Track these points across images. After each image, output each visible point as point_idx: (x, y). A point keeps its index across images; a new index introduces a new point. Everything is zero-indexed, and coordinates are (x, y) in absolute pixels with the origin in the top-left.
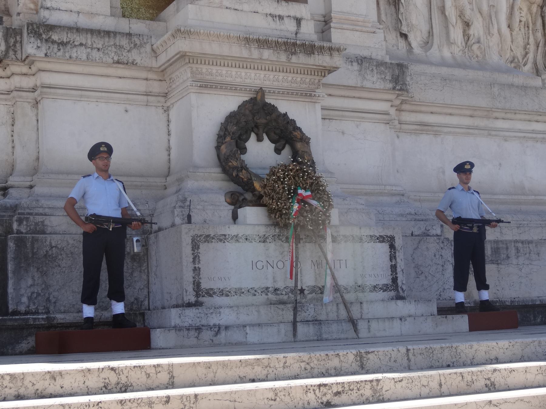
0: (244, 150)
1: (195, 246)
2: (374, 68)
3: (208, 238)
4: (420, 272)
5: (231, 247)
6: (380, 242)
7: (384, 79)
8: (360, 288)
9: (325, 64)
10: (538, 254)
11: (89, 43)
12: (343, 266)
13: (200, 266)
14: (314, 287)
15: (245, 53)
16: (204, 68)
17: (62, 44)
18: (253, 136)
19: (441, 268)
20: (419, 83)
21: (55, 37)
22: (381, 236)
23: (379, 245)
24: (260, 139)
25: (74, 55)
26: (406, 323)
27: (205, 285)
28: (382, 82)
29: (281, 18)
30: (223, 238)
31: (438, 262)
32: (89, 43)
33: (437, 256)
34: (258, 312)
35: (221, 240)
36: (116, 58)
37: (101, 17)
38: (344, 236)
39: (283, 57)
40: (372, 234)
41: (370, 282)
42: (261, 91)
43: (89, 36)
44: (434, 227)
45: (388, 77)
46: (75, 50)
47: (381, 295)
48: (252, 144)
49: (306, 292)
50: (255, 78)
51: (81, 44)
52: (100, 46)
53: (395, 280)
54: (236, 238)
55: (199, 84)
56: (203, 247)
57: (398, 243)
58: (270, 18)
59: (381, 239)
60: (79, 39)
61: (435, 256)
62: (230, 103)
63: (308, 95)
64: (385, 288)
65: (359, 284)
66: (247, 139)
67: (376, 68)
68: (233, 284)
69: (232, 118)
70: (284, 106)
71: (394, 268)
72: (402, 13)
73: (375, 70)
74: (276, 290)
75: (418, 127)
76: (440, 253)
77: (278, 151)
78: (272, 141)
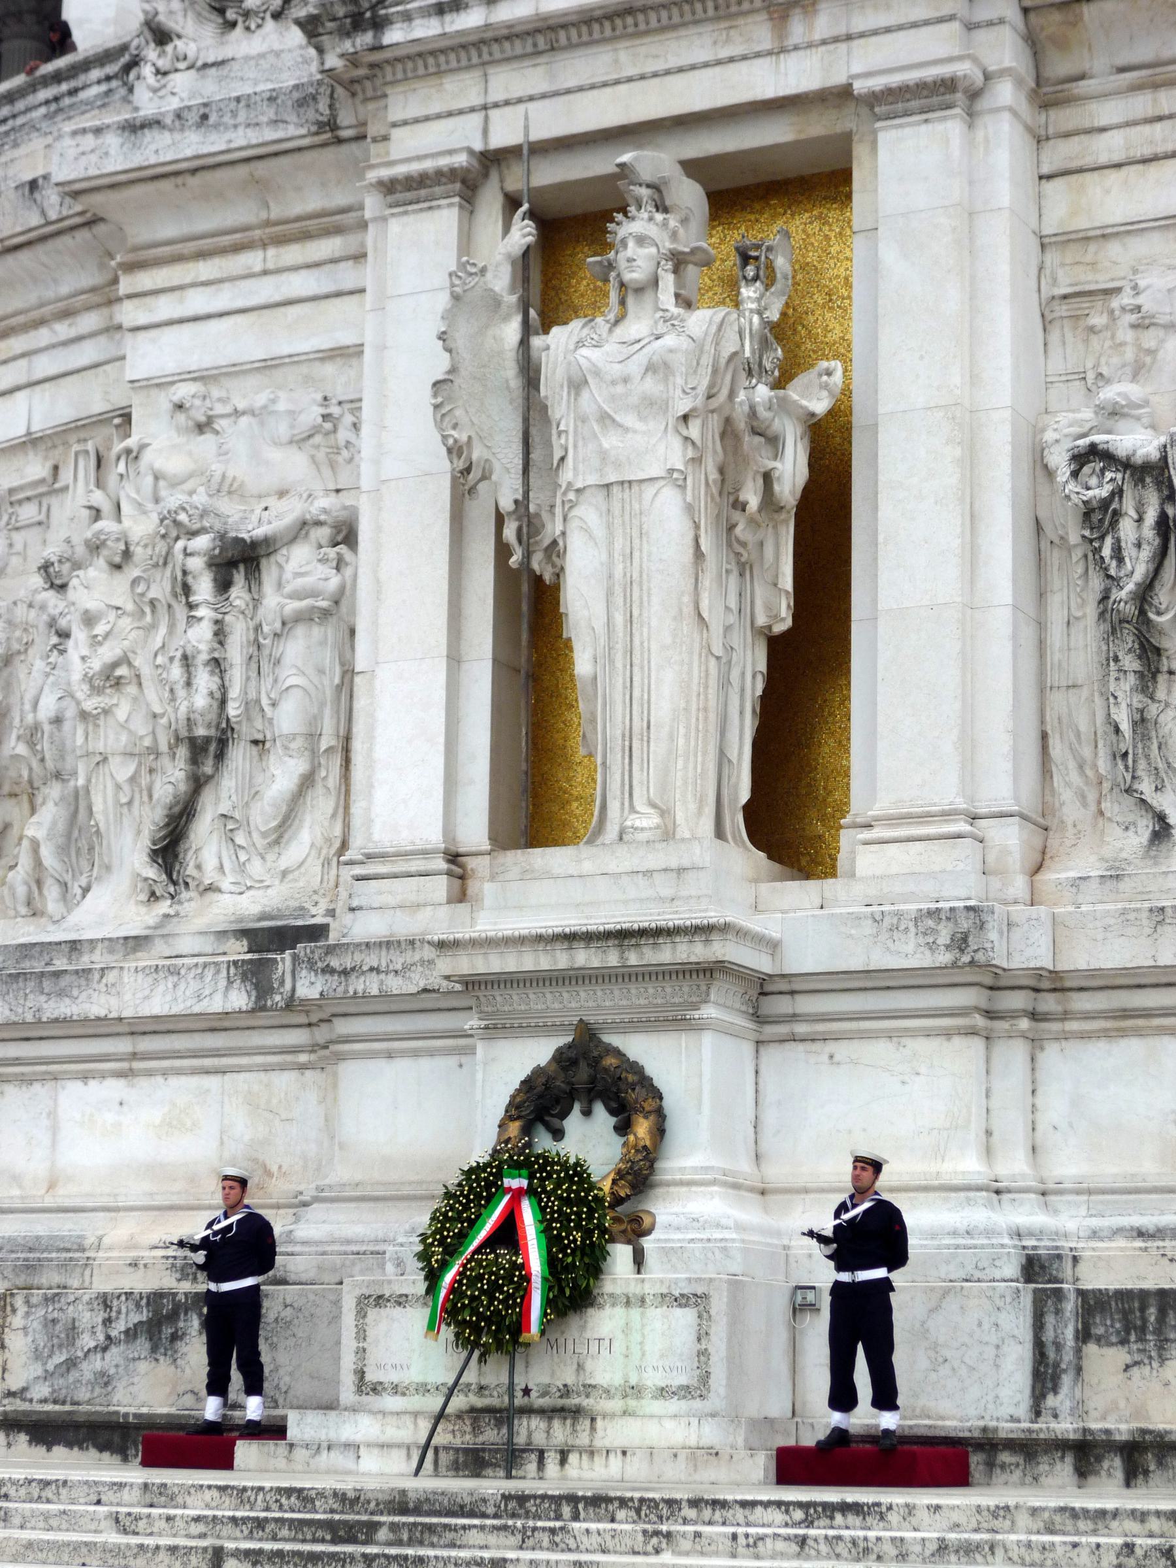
0: (558, 1134)
1: (361, 1314)
2: (911, 925)
4: (941, 1360)
6: (680, 1306)
7: (932, 947)
8: (634, 1391)
9: (693, 959)
11: (384, 964)
12: (605, 1352)
13: (365, 1345)
14: (549, 1385)
17: (345, 973)
18: (577, 1107)
19: (993, 1351)
20: (1091, 926)
21: (335, 963)
22: (682, 1295)
23: (678, 1312)
24: (587, 1113)
25: (360, 988)
26: (635, 1459)
27: (371, 1376)
28: (928, 953)
29: (648, 873)
31: (986, 1339)
32: (384, 964)
33: (986, 1326)
34: (416, 1424)
35: (400, 1304)
36: (422, 985)
37: (429, 908)
38: (611, 1295)
40: (665, 1291)
41: (653, 1379)
43: (384, 953)
44: (997, 1263)
45: (944, 938)
46: (362, 979)
47: (674, 1405)
48: (574, 1123)
49: (533, 1394)
51: (372, 969)
52: (399, 967)
53: (705, 1378)
55: (483, 1023)
56: (372, 1313)
58: (625, 880)
59: (682, 1301)
60: (371, 960)
61: (980, 1324)
64: (685, 1392)
65: (633, 1382)
66: (564, 1114)
67: (916, 926)
71: (703, 1354)
72: (1126, 754)
73: (913, 930)
74: (481, 1388)
75: (1109, 1024)
76: (993, 1319)
78: (612, 1112)
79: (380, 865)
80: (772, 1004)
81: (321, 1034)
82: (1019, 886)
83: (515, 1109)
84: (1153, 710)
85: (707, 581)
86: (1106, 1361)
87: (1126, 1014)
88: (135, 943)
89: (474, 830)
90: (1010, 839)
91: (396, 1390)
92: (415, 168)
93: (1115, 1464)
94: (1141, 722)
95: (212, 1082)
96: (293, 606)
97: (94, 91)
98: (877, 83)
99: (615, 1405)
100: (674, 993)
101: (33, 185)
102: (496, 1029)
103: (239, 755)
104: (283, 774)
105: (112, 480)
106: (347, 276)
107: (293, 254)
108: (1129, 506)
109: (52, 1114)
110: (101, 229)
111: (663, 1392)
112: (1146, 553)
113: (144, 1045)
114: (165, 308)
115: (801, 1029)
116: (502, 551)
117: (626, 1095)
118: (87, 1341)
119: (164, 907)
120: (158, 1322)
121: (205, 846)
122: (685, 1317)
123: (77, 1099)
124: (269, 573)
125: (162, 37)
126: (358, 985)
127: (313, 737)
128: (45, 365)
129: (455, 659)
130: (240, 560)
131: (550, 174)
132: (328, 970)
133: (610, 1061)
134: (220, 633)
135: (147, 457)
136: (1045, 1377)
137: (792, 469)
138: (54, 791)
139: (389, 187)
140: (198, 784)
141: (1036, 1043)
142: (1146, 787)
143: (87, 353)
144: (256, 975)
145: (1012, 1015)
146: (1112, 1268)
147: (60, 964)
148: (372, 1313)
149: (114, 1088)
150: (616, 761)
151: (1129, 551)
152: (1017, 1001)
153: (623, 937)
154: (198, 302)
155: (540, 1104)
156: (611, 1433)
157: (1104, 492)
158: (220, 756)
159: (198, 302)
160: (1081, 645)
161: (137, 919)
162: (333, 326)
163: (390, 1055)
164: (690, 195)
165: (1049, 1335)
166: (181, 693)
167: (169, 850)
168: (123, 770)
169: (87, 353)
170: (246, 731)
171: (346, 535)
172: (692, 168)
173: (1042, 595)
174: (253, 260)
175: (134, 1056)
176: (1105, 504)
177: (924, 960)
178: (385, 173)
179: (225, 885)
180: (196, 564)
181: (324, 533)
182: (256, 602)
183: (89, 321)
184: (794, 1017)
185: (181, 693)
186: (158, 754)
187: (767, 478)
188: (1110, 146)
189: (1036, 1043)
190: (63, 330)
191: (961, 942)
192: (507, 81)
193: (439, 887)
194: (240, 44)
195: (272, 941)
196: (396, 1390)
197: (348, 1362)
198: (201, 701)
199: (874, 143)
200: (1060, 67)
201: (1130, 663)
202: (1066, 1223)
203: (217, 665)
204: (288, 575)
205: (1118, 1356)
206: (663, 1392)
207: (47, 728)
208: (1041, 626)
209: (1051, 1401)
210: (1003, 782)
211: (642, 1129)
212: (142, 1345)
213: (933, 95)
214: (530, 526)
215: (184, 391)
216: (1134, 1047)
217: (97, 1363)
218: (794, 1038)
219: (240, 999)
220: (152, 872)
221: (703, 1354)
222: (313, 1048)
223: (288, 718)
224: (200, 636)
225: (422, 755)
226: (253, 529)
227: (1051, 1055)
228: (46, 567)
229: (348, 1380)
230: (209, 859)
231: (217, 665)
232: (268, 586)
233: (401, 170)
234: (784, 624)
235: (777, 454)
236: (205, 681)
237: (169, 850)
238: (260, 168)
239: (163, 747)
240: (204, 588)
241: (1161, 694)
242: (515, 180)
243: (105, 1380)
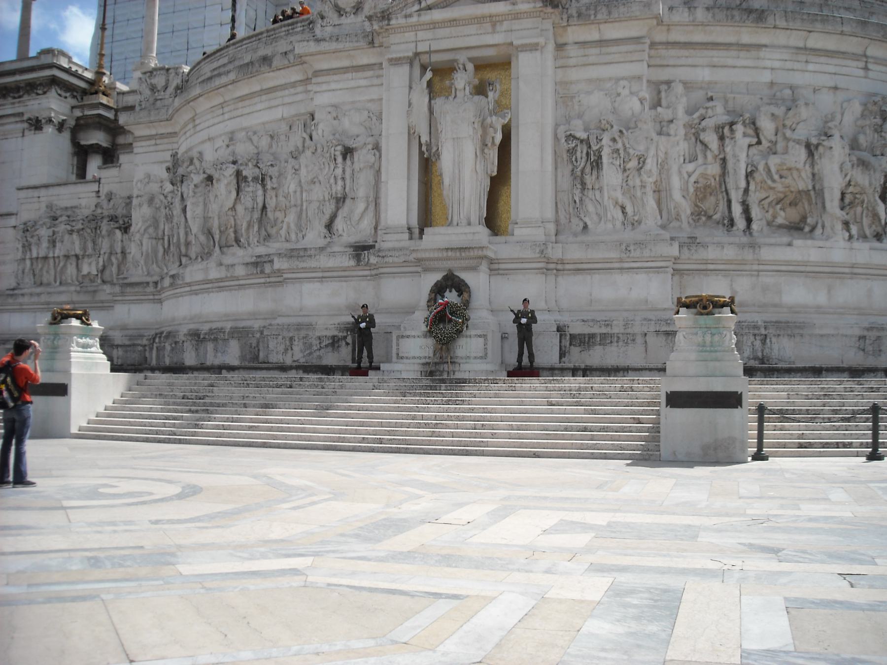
0: (443, 297)
1: (398, 340)
3: (403, 337)
5: (411, 340)
10: (634, 340)
15: (440, 255)
16: (427, 263)
24: (450, 291)
30: (408, 337)
39: (458, 254)
41: (473, 355)
42: (450, 270)
45: (538, 251)
47: (479, 361)
48: (447, 294)
50: (449, 264)
53: (486, 354)
54: (414, 337)
56: (400, 340)
57: (489, 337)
59: (480, 336)
62: (438, 277)
63: (474, 269)
64: (481, 358)
68: (411, 354)
69: (436, 284)
70: (463, 275)
71: (486, 348)
77: (459, 296)
79: (388, 230)
80: (495, 267)
81: (373, 272)
82: (553, 238)
83: (432, 291)
84: (584, 198)
85: (478, 162)
86: (575, 351)
87: (579, 270)
88: (322, 249)
89: (414, 222)
90: (552, 227)
91: (407, 358)
92: (398, 55)
93: (581, 373)
94: (581, 200)
95: (344, 284)
96: (362, 166)
97: (299, 29)
99: (464, 361)
101: (286, 53)
102: (426, 270)
103: (348, 201)
104: (361, 206)
105: (308, 131)
106: (376, 81)
107: (360, 74)
108: (579, 149)
110: (305, 65)
111: (475, 358)
112: (584, 160)
113: (324, 276)
114: (324, 87)
115: (501, 272)
116: (421, 153)
117: (461, 287)
118: (315, 348)
119: (328, 239)
120: (335, 343)
121: (339, 224)
122: (481, 340)
123: (307, 287)
124: (356, 155)
125: (323, 18)
126: (386, 259)
127: (367, 197)
128: (287, 100)
129: (409, 179)
130: (348, 152)
131: (435, 58)
132: (379, 256)
133: (456, 279)
134: (344, 171)
135: (321, 126)
136: (562, 354)
137: (499, 137)
138: (293, 210)
139: (390, 60)
140: (338, 209)
141: (556, 276)
142: (582, 216)
143: (300, 97)
144: (358, 258)
145: (552, 270)
146: (577, 329)
147: (302, 253)
148: (400, 340)
149: (317, 285)
150: (456, 207)
151: (579, 159)
152: (552, 266)
153: (461, 249)
154: (333, 86)
155: (439, 289)
156: (464, 367)
157: (574, 145)
158: (344, 202)
159: (333, 86)
160: (566, 181)
161: (322, 242)
162: (374, 93)
163: (394, 277)
164: (470, 67)
165: (563, 344)
166: (333, 186)
167: (329, 226)
168: (315, 205)
169: (300, 97)
170: (350, 196)
171: (377, 147)
172: (471, 60)
173: (556, 169)
174: (349, 75)
175: (323, 277)
176: (573, 148)
177: (533, 256)
178: (390, 56)
179: (345, 234)
180: (338, 153)
181: (370, 147)
182: (353, 163)
183: (300, 89)
184: (499, 269)
185: (333, 186)
186: (325, 201)
187: (493, 138)
188: (572, 62)
189: (556, 276)
190: (292, 91)
191: (542, 252)
192: (421, 35)
193: (407, 236)
194: (343, 20)
195: (360, 250)
196: (407, 358)
197: (394, 351)
198: (339, 188)
199: (517, 57)
200: (561, 41)
201: (579, 186)
202: (565, 319)
203: (343, 179)
204: (361, 157)
205: (578, 349)
206: (475, 358)
207: (292, 194)
208: (556, 176)
209: (563, 359)
210: (550, 214)
211: (465, 295)
212: (330, 349)
213: (533, 48)
214: (429, 145)
215: (329, 109)
216: (579, 278)
217: (318, 353)
218: (499, 274)
219: (352, 263)
220: (325, 231)
221: (486, 348)
222: (371, 276)
223: (361, 193)
224: (339, 171)
225: (399, 203)
226: (351, 144)
227: (560, 279)
228: (291, 153)
229: (394, 355)
230: (340, 229)
231: (343, 179)
232: (356, 159)
233: (394, 56)
234: (495, 173)
235: (495, 132)
236: (340, 183)
237: (329, 226)
238: (352, 53)
239: (327, 199)
240: (340, 159)
241: (586, 193)
242: (425, 59)
243: (320, 357)
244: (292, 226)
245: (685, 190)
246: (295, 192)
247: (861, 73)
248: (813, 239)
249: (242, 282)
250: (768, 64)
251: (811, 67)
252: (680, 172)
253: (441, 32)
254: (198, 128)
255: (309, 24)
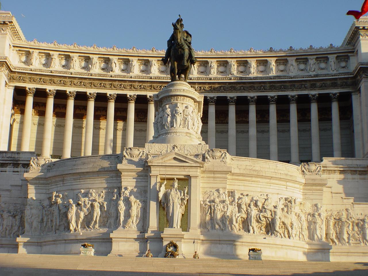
95: (133, 243)
98: (192, 175)
100: (180, 239)
109: (119, 245)
117: (175, 247)
123: (121, 243)
192: (161, 169)
244: (112, 223)
245: (237, 222)
246: (114, 213)
247: (285, 189)
248: (271, 237)
249: (91, 241)
250: (260, 186)
251: (271, 187)
252: (235, 216)
253: (168, 169)
254: (65, 185)
255: (118, 157)
